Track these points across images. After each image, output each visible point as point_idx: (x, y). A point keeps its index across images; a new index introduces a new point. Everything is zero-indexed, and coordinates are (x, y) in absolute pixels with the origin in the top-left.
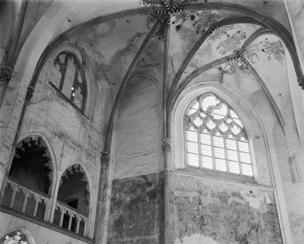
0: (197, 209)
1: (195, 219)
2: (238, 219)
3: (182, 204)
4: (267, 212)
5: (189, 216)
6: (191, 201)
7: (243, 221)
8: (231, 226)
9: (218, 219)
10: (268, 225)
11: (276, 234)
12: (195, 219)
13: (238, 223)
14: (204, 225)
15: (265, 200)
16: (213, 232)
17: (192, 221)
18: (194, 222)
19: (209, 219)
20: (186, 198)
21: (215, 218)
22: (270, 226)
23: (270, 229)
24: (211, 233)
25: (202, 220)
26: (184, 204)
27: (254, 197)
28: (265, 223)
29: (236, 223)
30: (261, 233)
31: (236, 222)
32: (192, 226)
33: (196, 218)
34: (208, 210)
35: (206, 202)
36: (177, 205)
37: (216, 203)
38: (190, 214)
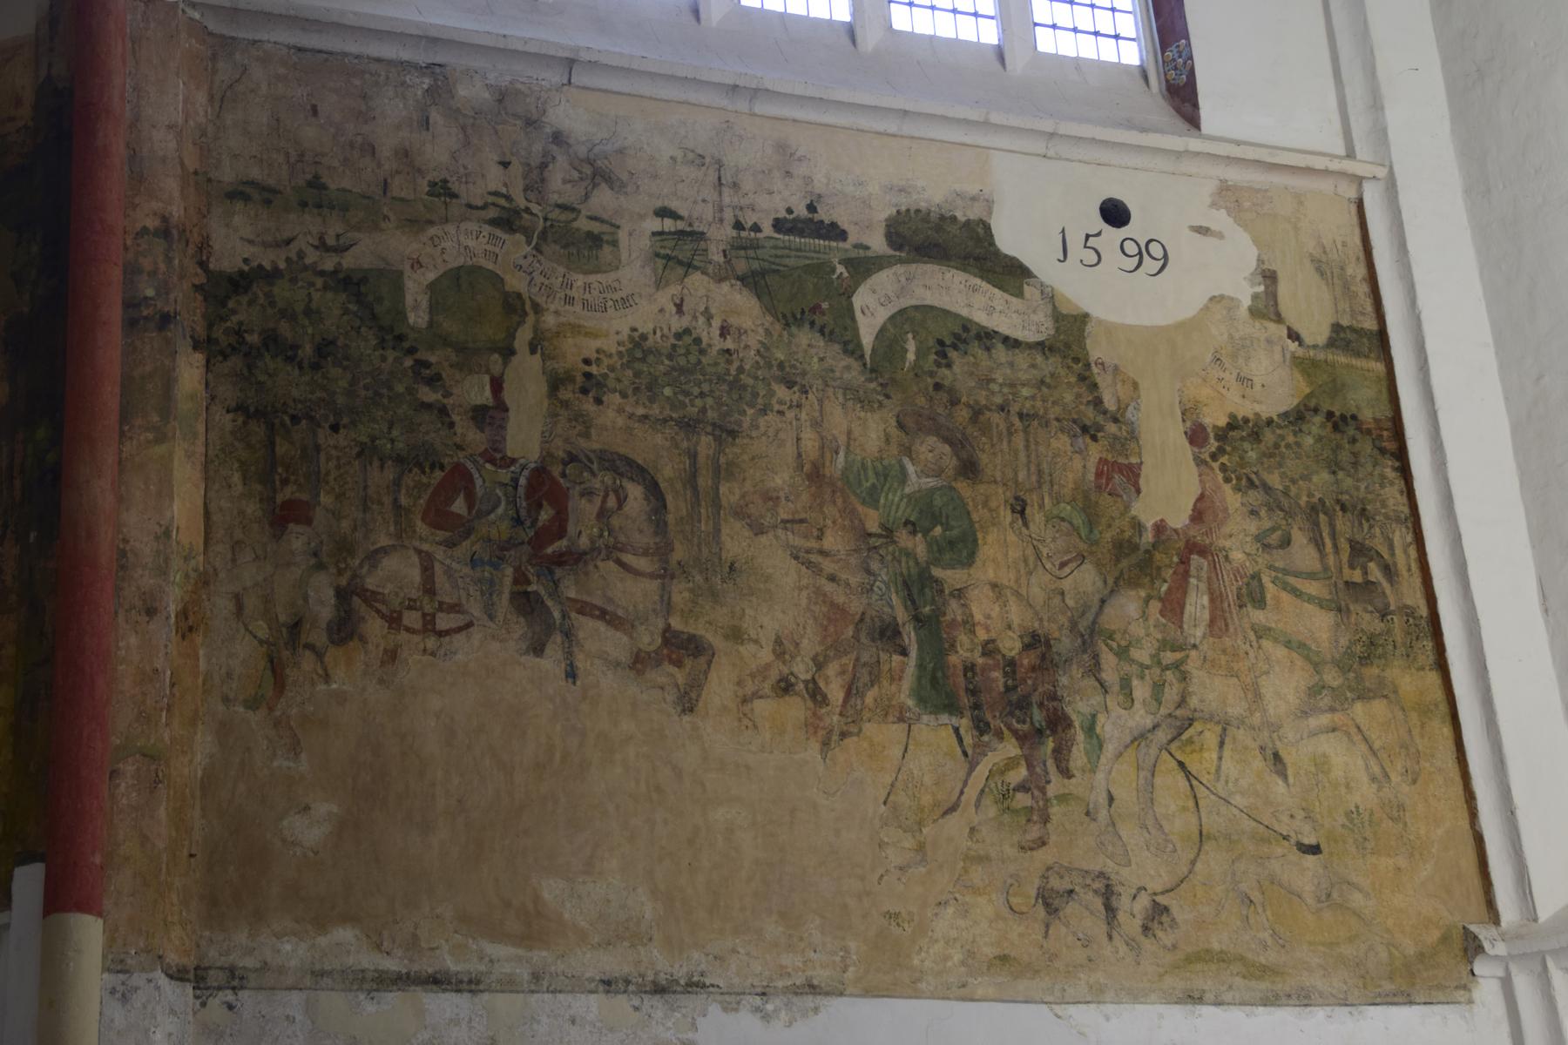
0: (485, 396)
1: (459, 506)
2: (962, 487)
3: (307, 350)
4: (1285, 415)
5: (380, 477)
6: (417, 317)
7: (1022, 512)
8: (875, 566)
9: (730, 493)
10: (1300, 538)
11: (1378, 626)
12: (459, 506)
13: (955, 532)
14: (560, 560)
15: (1272, 295)
16: (668, 628)
17: (421, 528)
18: (441, 535)
19: (620, 507)
20: (350, 283)
21: (695, 489)
22: (1319, 544)
23: (1311, 576)
24: (648, 639)
25: (545, 515)
26: (325, 348)
27: (1150, 265)
28: (1267, 524)
29: (938, 530)
30: (1218, 623)
31: (936, 519)
32: (415, 575)
33: (470, 504)
34: (620, 410)
35: (590, 321)
36: (236, 362)
37: (710, 335)
38: (399, 460)
